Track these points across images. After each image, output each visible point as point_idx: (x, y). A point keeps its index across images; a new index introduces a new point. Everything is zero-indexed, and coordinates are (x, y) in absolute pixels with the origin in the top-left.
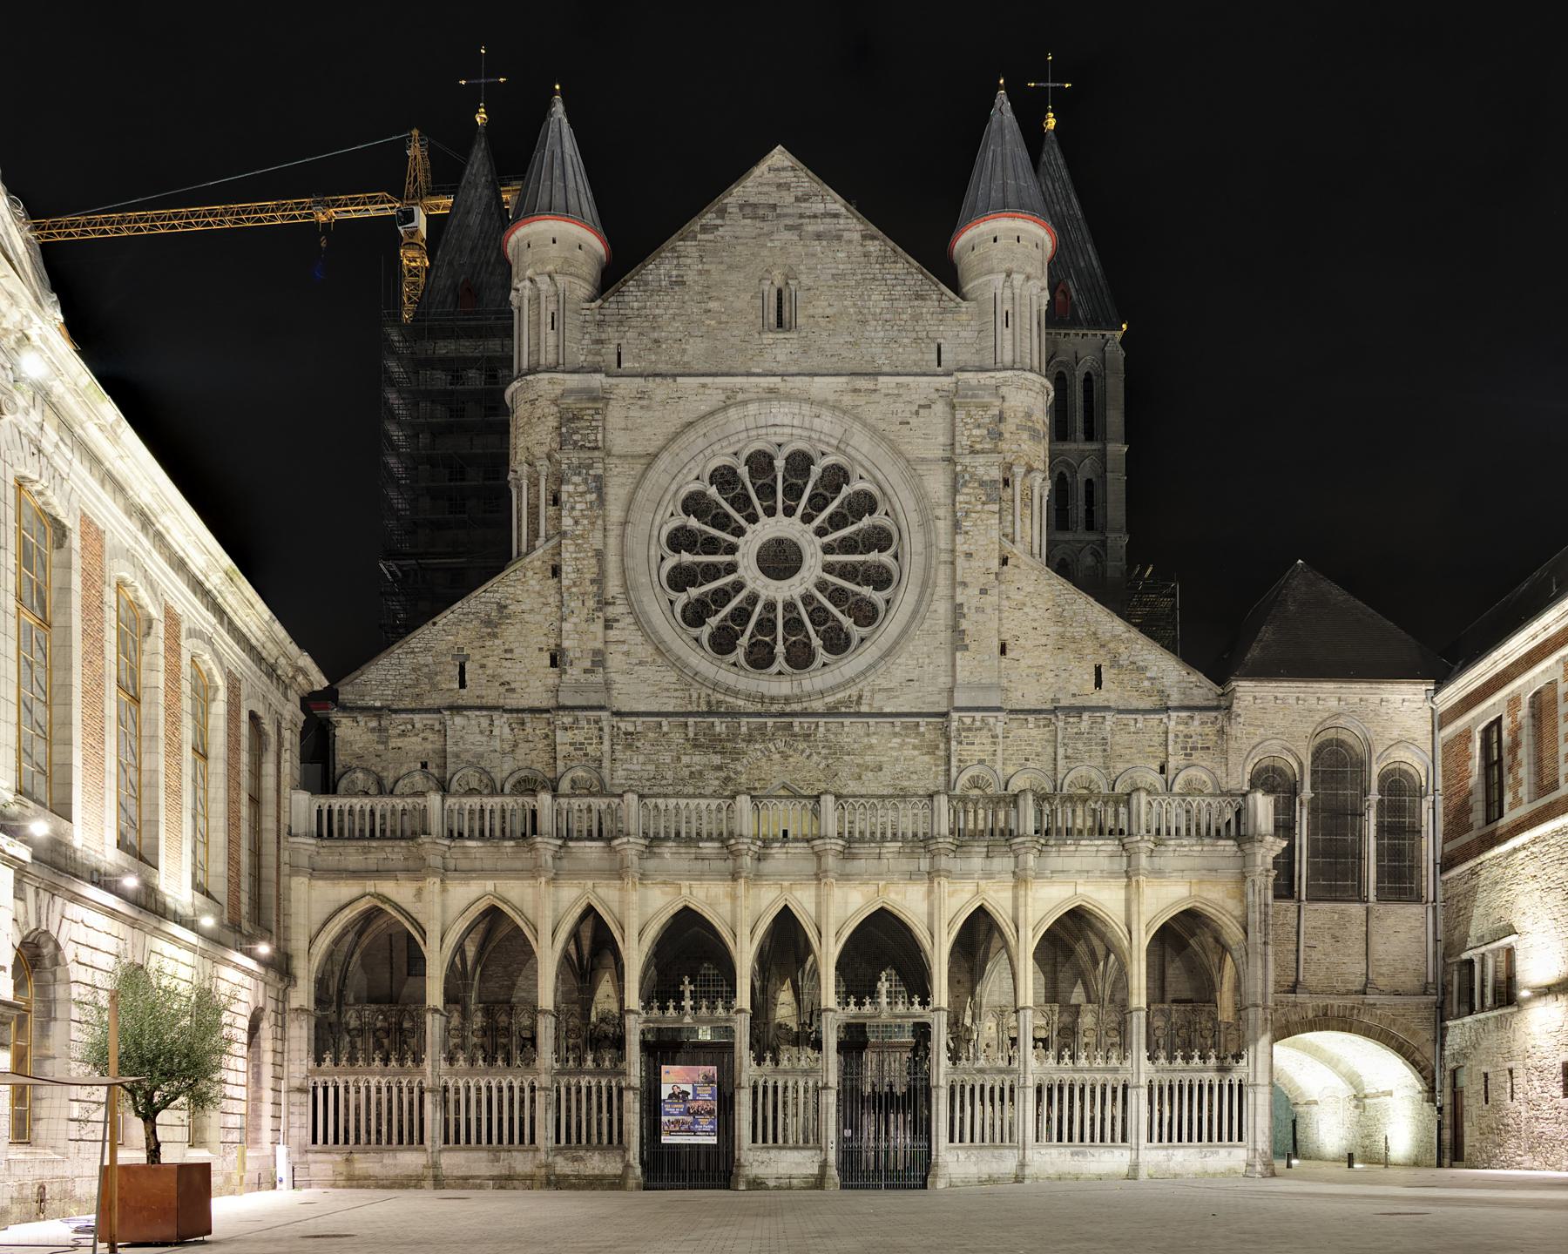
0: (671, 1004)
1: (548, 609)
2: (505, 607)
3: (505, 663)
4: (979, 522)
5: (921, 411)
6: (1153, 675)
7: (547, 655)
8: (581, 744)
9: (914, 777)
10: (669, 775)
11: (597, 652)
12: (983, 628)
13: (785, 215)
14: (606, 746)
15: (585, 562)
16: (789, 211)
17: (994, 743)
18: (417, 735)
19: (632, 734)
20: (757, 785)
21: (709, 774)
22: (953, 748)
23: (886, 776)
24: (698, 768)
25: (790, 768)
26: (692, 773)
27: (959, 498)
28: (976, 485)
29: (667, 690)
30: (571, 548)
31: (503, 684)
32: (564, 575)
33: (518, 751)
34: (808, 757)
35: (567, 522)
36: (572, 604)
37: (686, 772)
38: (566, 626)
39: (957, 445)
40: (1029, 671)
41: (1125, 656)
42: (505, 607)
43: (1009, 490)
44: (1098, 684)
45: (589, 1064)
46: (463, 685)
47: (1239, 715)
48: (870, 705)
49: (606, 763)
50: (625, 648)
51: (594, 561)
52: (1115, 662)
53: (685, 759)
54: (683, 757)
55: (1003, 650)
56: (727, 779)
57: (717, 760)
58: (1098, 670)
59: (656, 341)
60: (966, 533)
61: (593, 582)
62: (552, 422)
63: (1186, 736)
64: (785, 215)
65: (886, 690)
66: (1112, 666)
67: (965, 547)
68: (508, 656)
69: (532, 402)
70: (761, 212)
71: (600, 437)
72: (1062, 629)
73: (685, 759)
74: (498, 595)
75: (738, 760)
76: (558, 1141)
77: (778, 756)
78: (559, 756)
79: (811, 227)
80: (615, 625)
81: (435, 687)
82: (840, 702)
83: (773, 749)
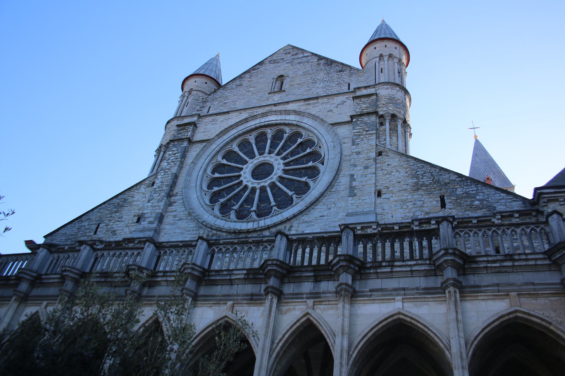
5: (339, 106)
7: (136, 218)
13: (286, 60)
15: (166, 178)
29: (189, 231)
36: (155, 195)
40: (395, 203)
43: (384, 127)
50: (175, 213)
55: (379, 194)
59: (226, 103)
60: (358, 144)
64: (286, 60)
67: (357, 150)
72: (417, 180)
80: (174, 204)
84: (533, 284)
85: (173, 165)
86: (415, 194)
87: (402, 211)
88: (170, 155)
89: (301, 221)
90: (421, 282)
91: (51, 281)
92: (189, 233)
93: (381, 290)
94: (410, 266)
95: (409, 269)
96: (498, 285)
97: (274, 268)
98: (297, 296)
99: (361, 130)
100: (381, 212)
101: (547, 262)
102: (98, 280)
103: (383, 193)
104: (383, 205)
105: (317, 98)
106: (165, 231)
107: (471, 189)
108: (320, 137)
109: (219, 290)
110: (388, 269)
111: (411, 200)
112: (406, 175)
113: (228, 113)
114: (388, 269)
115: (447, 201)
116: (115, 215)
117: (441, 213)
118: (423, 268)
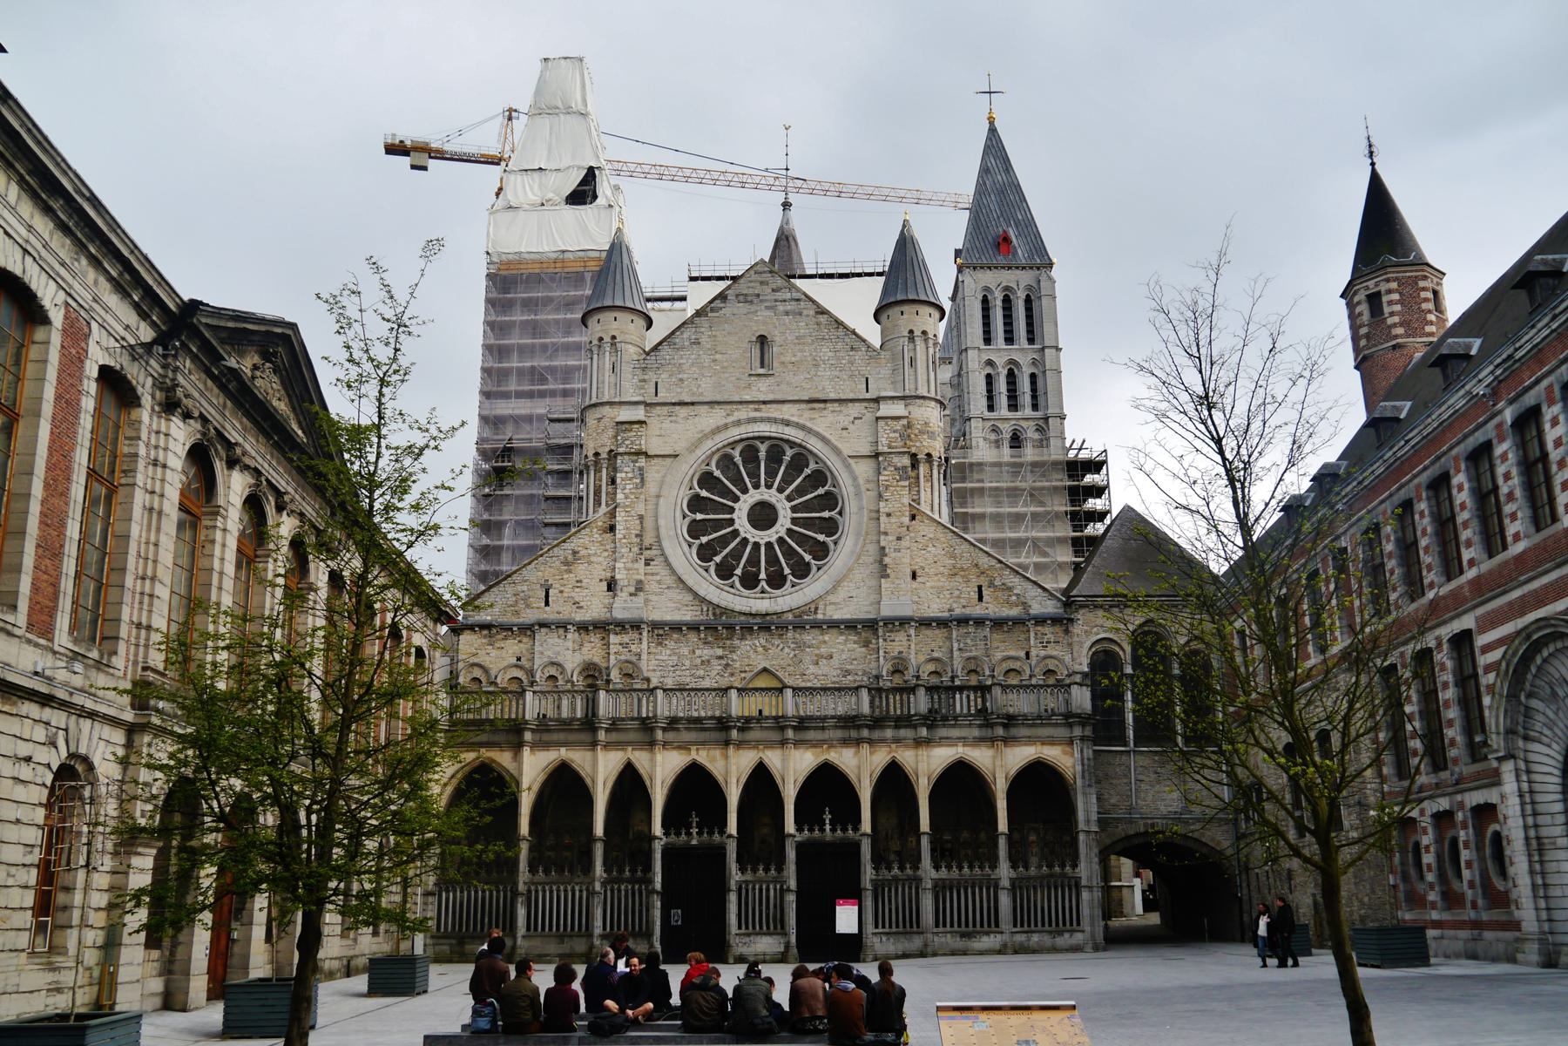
1: (606, 554)
7: (605, 583)
10: (687, 663)
11: (640, 582)
12: (901, 560)
14: (645, 645)
16: (768, 297)
21: (714, 662)
23: (835, 662)
30: (623, 514)
35: (620, 496)
37: (698, 661)
38: (617, 565)
44: (981, 598)
46: (547, 604)
49: (644, 657)
50: (658, 578)
53: (698, 652)
55: (914, 576)
56: (727, 665)
57: (720, 652)
58: (980, 587)
59: (681, 380)
61: (637, 536)
62: (611, 433)
67: (887, 510)
69: (599, 420)
70: (749, 299)
73: (698, 652)
76: (604, 929)
78: (612, 651)
79: (781, 308)
81: (528, 606)
90: (976, 732)
98: (883, 741)
105: (825, 401)
108: (836, 473)
113: (693, 404)
115: (984, 593)
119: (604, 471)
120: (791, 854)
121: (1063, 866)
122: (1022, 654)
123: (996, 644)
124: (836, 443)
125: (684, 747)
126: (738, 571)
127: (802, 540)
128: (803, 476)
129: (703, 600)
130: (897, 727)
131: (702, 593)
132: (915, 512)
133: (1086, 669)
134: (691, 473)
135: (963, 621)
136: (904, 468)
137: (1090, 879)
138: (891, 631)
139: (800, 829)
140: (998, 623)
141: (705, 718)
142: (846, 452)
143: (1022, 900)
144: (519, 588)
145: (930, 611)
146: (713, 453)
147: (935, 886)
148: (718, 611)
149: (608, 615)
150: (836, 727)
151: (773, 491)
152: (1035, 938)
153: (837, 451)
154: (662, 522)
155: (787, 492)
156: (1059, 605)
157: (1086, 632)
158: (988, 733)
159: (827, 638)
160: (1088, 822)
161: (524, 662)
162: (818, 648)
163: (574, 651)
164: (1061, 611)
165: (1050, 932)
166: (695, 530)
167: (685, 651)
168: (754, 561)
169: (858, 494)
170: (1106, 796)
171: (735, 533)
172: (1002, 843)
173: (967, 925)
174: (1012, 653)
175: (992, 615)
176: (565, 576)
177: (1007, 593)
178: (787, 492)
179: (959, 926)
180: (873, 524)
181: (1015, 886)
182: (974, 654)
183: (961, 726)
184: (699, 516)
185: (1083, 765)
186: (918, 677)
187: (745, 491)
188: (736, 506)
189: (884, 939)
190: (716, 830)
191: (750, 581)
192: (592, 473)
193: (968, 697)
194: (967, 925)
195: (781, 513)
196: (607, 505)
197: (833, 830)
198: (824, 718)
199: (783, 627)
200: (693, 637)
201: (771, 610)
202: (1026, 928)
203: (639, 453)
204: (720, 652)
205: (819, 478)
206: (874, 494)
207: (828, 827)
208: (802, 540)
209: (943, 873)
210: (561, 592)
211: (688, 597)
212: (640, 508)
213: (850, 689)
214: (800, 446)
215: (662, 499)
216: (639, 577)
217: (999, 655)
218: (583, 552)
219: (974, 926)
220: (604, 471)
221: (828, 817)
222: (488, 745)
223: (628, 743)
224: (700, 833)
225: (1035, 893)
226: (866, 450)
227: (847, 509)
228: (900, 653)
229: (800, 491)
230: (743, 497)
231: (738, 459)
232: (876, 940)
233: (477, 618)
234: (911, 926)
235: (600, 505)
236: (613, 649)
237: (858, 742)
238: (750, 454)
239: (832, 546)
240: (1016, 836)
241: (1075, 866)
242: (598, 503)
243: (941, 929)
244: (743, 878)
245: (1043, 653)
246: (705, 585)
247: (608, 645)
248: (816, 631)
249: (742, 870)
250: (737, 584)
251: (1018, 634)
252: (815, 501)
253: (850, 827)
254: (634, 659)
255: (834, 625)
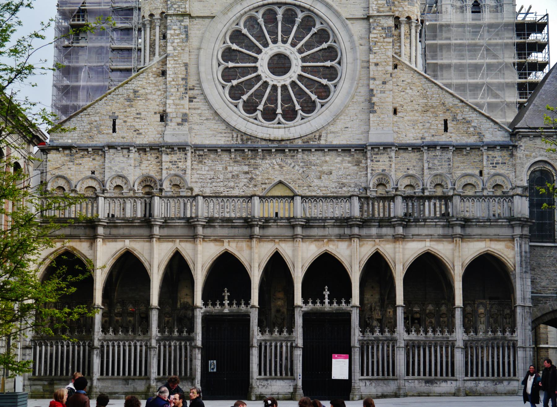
0: (218, 303)
1: (159, 93)
2: (138, 92)
3: (137, 120)
4: (382, 47)
6: (475, 125)
7: (158, 116)
8: (176, 162)
9: (349, 177)
10: (221, 177)
11: (185, 115)
17: (390, 161)
18: (90, 157)
19: (202, 156)
20: (267, 181)
21: (242, 176)
22: (368, 164)
23: (334, 177)
24: (236, 173)
25: (284, 173)
26: (233, 175)
27: (371, 36)
28: (380, 28)
29: (221, 133)
30: (172, 62)
31: (135, 131)
32: (168, 76)
33: (142, 165)
34: (293, 167)
35: (170, 48)
36: (172, 90)
37: (230, 175)
39: (370, 9)
40: (408, 123)
41: (460, 115)
42: (138, 92)
44: (446, 129)
45: (176, 334)
46: (114, 131)
47: (521, 146)
48: (326, 140)
49: (189, 172)
50: (199, 111)
51: (184, 68)
52: (454, 119)
53: (230, 169)
54: (228, 168)
55: (395, 112)
56: (252, 179)
57: (246, 169)
58: (446, 121)
60: (375, 53)
61: (183, 79)
63: (493, 157)
65: (333, 132)
66: (453, 121)
67: (375, 61)
68: (138, 116)
71: (187, 6)
72: (426, 101)
74: (133, 85)
75: (257, 168)
76: (159, 374)
77: (277, 167)
80: (194, 100)
81: (100, 132)
82: (310, 139)
83: (275, 163)
84: (498, 235)
85: (181, 51)
86: (425, 115)
87: (413, 131)
88: (172, 35)
89: (329, 131)
90: (440, 231)
91: (177, 224)
92: (222, 135)
93: (418, 235)
94: (435, 222)
95: (434, 223)
96: (481, 235)
97: (358, 223)
98: (369, 237)
99: (379, 36)
100: (397, 130)
101: (508, 223)
102: (220, 224)
103: (398, 111)
104: (399, 123)
106: (194, 131)
107: (467, 116)
109: (315, 232)
110: (423, 223)
111: (421, 121)
112: (418, 94)
114: (423, 223)
116: (130, 110)
117: (443, 136)
118: (442, 223)
119: (157, 29)
120: (299, 321)
121: (504, 332)
122: (477, 172)
123: (456, 164)
124: (337, 8)
125: (219, 240)
126: (261, 107)
127: (310, 83)
128: (311, 33)
129: (233, 129)
130: (380, 226)
131: (233, 124)
132: (396, 62)
133: (526, 184)
134: (224, 30)
135: (432, 147)
136: (389, 28)
137: (524, 342)
138: (377, 154)
139: (306, 302)
140: (459, 149)
141: (236, 218)
142: (345, 15)
143: (472, 356)
144: (93, 118)
145: (407, 138)
146: (242, 16)
147: (407, 346)
148: (245, 137)
149: (161, 140)
150: (334, 226)
151: (288, 45)
152: (482, 384)
153: (337, 14)
154: (202, 69)
155: (299, 46)
156: (506, 134)
157: (527, 155)
158: (449, 231)
159: (327, 158)
160: (524, 299)
161: (97, 175)
162: (321, 166)
163: (135, 167)
164: (508, 139)
165: (493, 381)
166: (228, 75)
167: (220, 167)
168: (272, 99)
169: (353, 48)
170: (538, 280)
171: (258, 78)
172: (458, 314)
173: (430, 375)
174: (469, 171)
175: (455, 143)
176: (128, 110)
177: (466, 125)
178: (299, 46)
179: (425, 375)
180: (364, 72)
181: (467, 346)
182: (438, 172)
183: (429, 226)
184: (231, 65)
185: (521, 256)
186: (397, 189)
187: (266, 45)
188: (259, 56)
189: (368, 383)
190: (243, 302)
191: (269, 115)
192: (148, 30)
193: (435, 204)
194: (430, 375)
195: (294, 62)
196: (160, 55)
197: (331, 303)
198: (325, 220)
199: (294, 150)
200: (225, 156)
201: (285, 137)
202: (475, 377)
203: (184, 15)
204: (246, 169)
205: (323, 35)
206: (365, 48)
207: (327, 301)
208: (310, 83)
209: (413, 336)
210: (125, 122)
211: (223, 127)
212: (185, 58)
213: (345, 197)
214: (309, 10)
215: (202, 51)
216: (184, 111)
217: (459, 173)
218: (141, 91)
219: (436, 375)
220: (157, 29)
221: (327, 293)
222: (71, 237)
223: (177, 237)
224: (230, 304)
225: (482, 352)
226: (360, 13)
227: (344, 60)
228: (383, 170)
229: (308, 46)
230: (264, 50)
231: (261, 21)
232: (362, 384)
233: (61, 141)
234: (388, 375)
235: (154, 55)
236: (165, 166)
237: (351, 237)
238: (270, 17)
239: (332, 88)
240: (469, 309)
241: (513, 332)
242: (153, 53)
243: (411, 377)
244: (263, 338)
245: (493, 171)
246: (235, 117)
247: (161, 162)
248: (320, 153)
249: (262, 331)
250: (260, 117)
251: (474, 157)
252: (320, 54)
253: (343, 301)
254: (181, 173)
255: (333, 149)
